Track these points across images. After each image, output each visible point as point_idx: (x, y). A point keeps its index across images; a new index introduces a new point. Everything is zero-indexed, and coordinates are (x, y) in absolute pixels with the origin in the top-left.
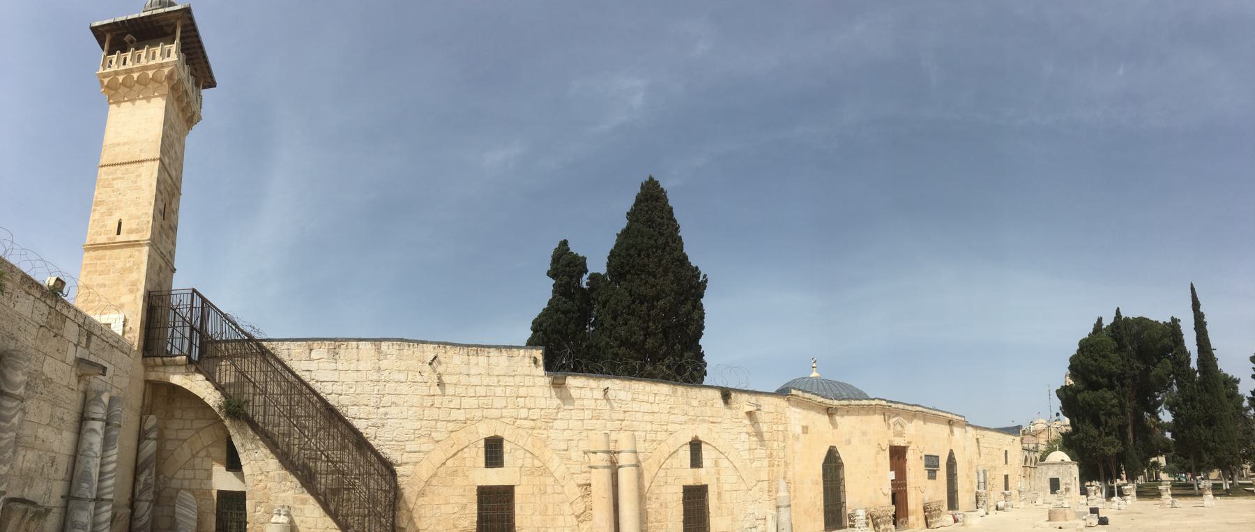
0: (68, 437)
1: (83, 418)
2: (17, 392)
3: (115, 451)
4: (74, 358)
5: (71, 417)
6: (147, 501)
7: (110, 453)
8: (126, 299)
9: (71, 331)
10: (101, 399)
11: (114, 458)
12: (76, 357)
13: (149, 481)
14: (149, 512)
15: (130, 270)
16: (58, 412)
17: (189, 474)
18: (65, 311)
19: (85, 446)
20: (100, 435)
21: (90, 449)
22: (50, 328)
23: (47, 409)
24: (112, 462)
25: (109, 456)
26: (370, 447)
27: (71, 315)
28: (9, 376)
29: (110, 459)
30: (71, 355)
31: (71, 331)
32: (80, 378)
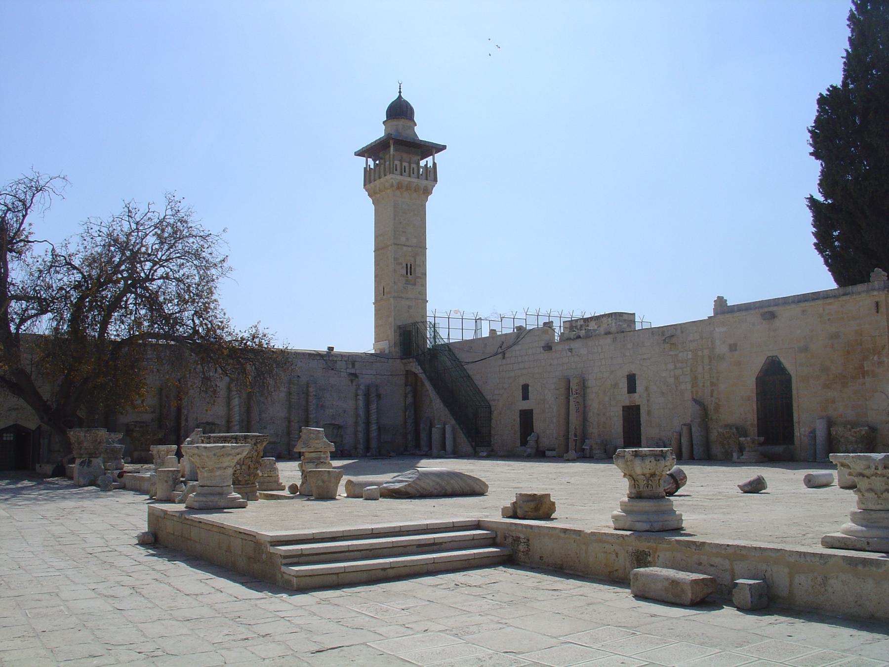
11: (374, 408)
18: (335, 359)
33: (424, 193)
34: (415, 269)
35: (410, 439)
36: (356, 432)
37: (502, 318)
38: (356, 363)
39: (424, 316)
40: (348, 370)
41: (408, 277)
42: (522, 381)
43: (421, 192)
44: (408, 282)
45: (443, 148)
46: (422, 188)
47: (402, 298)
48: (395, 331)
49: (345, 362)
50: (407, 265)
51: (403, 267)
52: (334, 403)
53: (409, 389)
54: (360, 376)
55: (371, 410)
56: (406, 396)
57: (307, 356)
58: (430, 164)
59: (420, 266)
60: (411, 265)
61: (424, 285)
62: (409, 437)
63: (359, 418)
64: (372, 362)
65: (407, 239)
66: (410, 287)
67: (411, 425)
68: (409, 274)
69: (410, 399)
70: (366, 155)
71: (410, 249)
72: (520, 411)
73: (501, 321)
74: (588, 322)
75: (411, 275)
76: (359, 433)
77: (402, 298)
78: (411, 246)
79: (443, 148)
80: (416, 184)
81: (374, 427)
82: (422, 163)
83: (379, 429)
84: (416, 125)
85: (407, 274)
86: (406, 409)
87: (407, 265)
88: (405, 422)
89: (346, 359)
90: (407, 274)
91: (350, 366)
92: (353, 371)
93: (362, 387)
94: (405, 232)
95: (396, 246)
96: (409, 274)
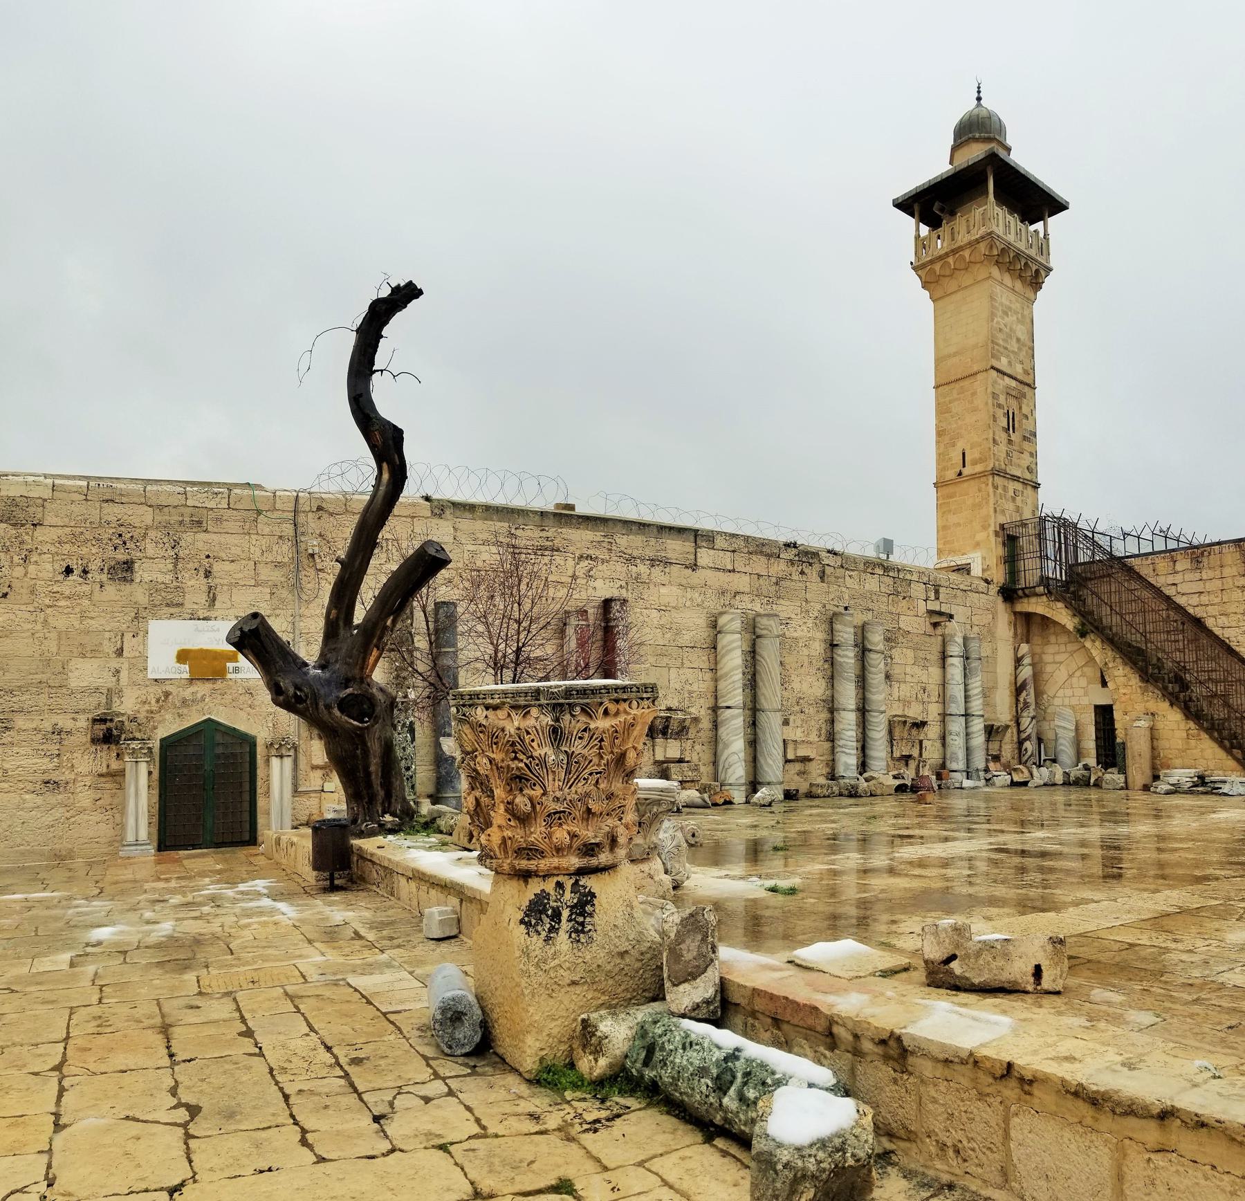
0: (935, 671)
2: (878, 648)
3: (978, 678)
5: (935, 656)
7: (973, 680)
8: (981, 536)
9: (918, 590)
11: (979, 684)
15: (980, 506)
16: (921, 654)
17: (1068, 692)
18: (908, 577)
19: (949, 676)
22: (897, 594)
23: (910, 653)
27: (915, 577)
28: (870, 638)
31: (918, 590)
32: (935, 625)
34: (1020, 422)
35: (1029, 753)
38: (942, 590)
41: (1009, 436)
52: (908, 670)
57: (862, 566)
63: (953, 705)
69: (1026, 672)
76: (956, 738)
81: (978, 726)
94: (1006, 348)
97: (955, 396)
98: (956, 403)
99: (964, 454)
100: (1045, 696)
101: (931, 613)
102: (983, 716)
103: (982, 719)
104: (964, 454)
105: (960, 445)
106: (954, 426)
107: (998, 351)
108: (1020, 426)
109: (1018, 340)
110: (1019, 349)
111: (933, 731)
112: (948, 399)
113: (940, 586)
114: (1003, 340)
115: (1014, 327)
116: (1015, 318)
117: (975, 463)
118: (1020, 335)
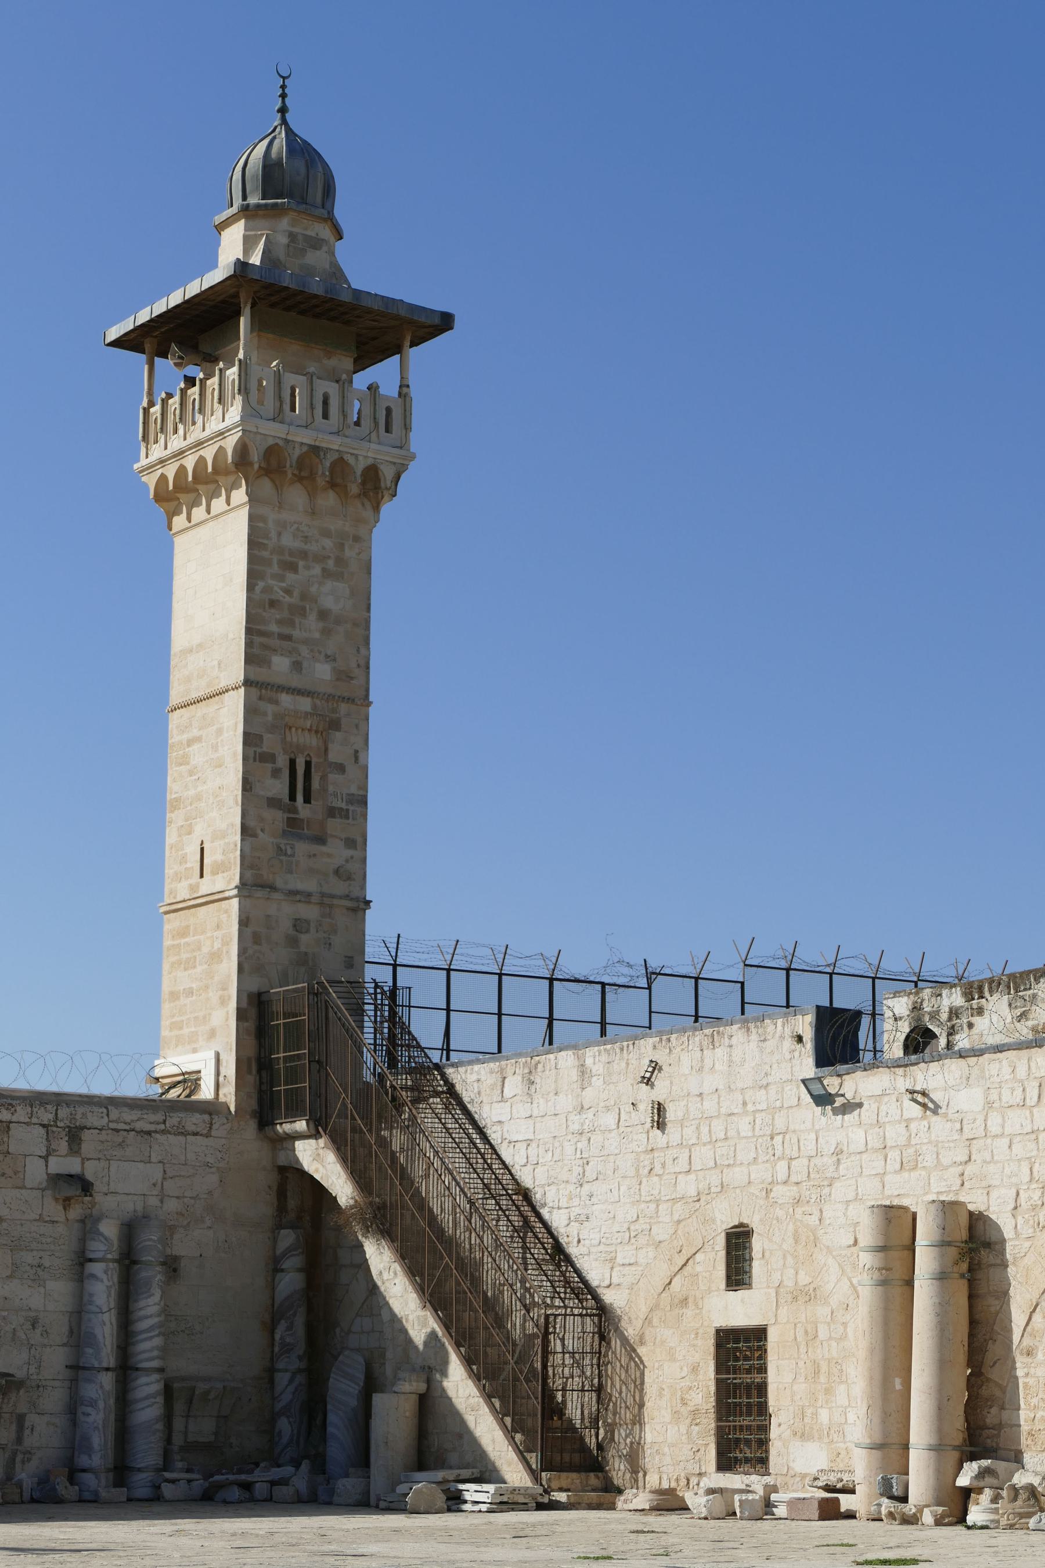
1: (82, 1260)
4: (45, 1177)
6: (286, 1371)
7: (142, 1303)
10: (98, 1229)
11: (154, 1309)
12: (48, 1174)
13: (288, 1340)
14: (291, 1388)
20: (102, 1281)
21: (91, 1303)
24: (147, 1317)
25: (140, 1309)
26: (568, 1259)
29: (142, 1313)
30: (36, 1172)
33: (364, 494)
35: (285, 1440)
36: (73, 1408)
37: (651, 976)
38: (86, 1135)
39: (354, 958)
40: (52, 1160)
41: (295, 811)
42: (725, 1219)
43: (354, 489)
44: (294, 826)
45: (444, 322)
46: (359, 472)
47: (273, 888)
48: (241, 1015)
49: (42, 1131)
50: (292, 763)
51: (276, 773)
53: (287, 1238)
54: (99, 1187)
55: (141, 1319)
56: (275, 1267)
58: (389, 389)
59: (341, 768)
60: (308, 764)
61: (357, 843)
62: (284, 1425)
63: (89, 1351)
64: (149, 1133)
65: (297, 666)
66: (302, 848)
67: (291, 1381)
68: (300, 798)
69: (290, 1282)
70: (147, 347)
71: (305, 704)
72: (718, 1331)
73: (649, 988)
74: (981, 997)
75: (307, 800)
76: (89, 1410)
77: (273, 888)
78: (308, 694)
79: (444, 322)
80: (336, 456)
82: (361, 380)
83: (168, 1392)
84: (341, 238)
85: (292, 797)
86: (274, 1317)
87: (292, 763)
88: (271, 1371)
89: (47, 1117)
90: (292, 797)
91: (63, 1146)
92: (72, 1165)
93: (109, 1229)
94: (288, 638)
95: (254, 690)
96: (300, 798)
97: (195, 732)
98: (196, 747)
99: (202, 849)
100: (338, 1330)
101: (57, 1180)
102: (161, 1370)
103: (155, 1377)
104: (202, 849)
105: (200, 831)
106: (192, 792)
107: (265, 647)
108: (324, 789)
109: (323, 615)
110: (327, 632)
111: (54, 1398)
112: (185, 737)
113: (83, 1128)
114: (280, 622)
115: (313, 589)
116: (317, 570)
117: (219, 869)
118: (328, 602)
